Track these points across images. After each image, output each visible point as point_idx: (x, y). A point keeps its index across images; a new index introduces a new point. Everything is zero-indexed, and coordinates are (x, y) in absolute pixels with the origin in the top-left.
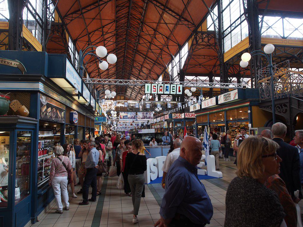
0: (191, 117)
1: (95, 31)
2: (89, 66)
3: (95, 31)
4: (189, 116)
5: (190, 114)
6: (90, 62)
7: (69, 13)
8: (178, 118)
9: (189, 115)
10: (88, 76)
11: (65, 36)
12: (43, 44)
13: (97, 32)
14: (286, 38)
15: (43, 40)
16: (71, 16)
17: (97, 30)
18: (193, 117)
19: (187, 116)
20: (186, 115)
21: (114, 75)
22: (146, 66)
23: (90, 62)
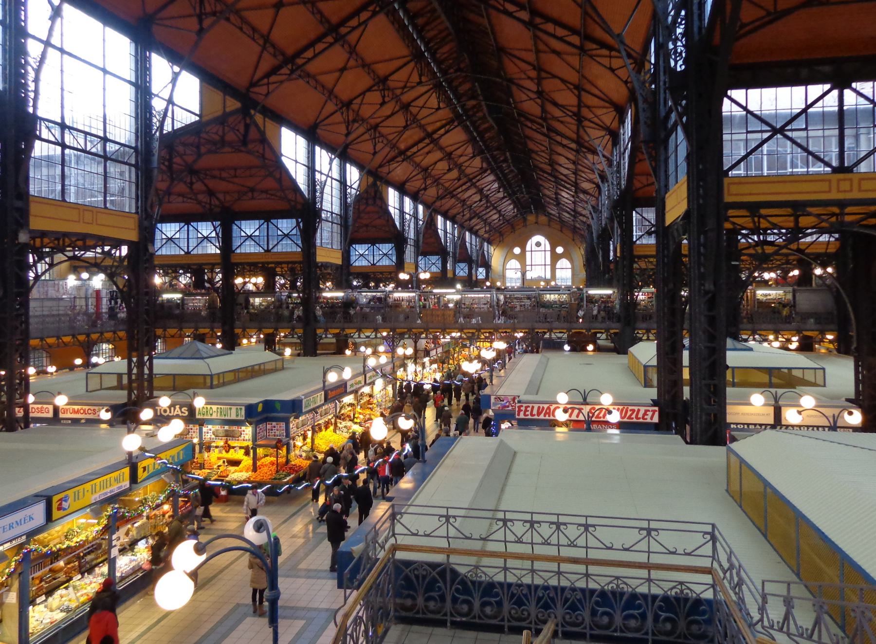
0: (536, 417)
1: (363, 94)
2: (388, 172)
3: (363, 94)
4: (527, 413)
5: (533, 407)
6: (389, 162)
7: (259, 74)
8: (510, 408)
9: (529, 409)
10: (392, 196)
11: (263, 133)
12: (139, 210)
13: (368, 94)
14: (849, 170)
15: (140, 202)
16: (265, 81)
17: (369, 90)
18: (542, 417)
19: (522, 413)
20: (520, 411)
21: (486, 174)
22: (565, 155)
23: (389, 162)
